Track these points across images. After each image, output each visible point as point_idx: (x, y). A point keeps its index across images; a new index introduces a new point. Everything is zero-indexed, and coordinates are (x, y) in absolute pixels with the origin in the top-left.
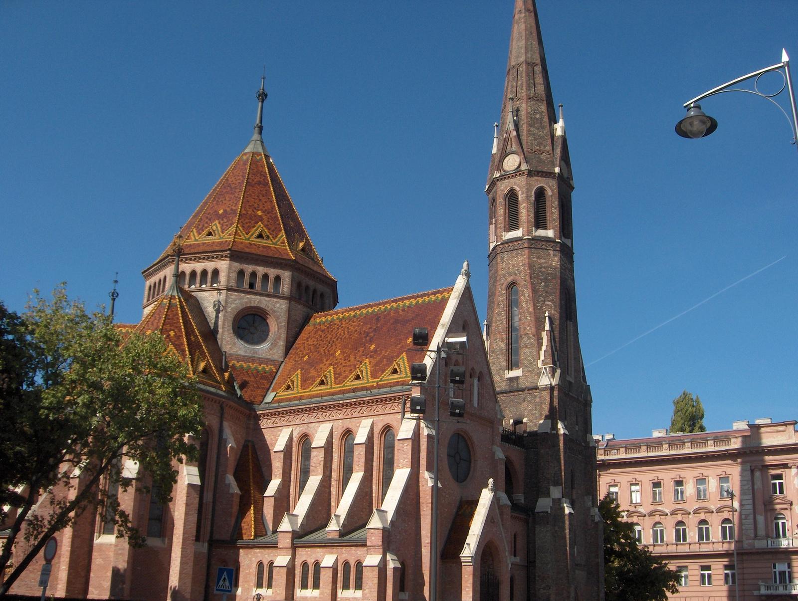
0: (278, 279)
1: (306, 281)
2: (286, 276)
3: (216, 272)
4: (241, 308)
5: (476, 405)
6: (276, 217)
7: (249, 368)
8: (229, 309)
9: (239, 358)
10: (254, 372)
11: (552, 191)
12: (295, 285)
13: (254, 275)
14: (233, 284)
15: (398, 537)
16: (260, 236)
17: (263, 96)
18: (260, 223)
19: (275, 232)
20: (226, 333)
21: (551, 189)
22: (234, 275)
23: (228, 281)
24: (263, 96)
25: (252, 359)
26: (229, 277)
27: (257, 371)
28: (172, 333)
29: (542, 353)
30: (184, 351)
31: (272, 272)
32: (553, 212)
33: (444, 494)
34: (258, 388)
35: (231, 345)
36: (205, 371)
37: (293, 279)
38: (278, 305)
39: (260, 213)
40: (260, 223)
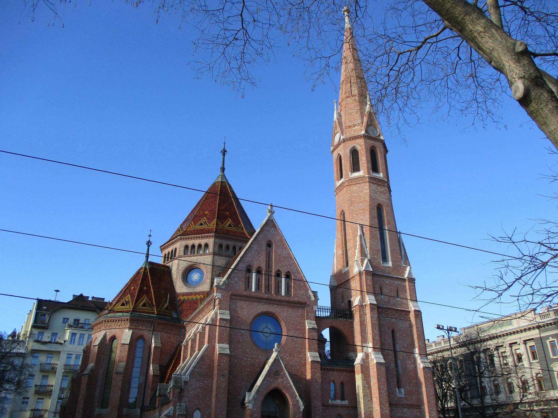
0: (207, 245)
1: (225, 243)
2: (211, 241)
3: (176, 249)
4: (186, 266)
5: (283, 294)
6: (215, 212)
7: (188, 299)
8: (180, 268)
9: (184, 294)
10: (190, 300)
11: (361, 146)
12: (217, 246)
13: (193, 246)
14: (182, 254)
15: (191, 393)
16: (201, 224)
17: (224, 152)
18: (205, 218)
19: (210, 220)
20: (178, 282)
21: (361, 145)
22: (182, 249)
23: (179, 253)
24: (224, 152)
25: (191, 294)
26: (179, 250)
27: (192, 299)
28: (133, 287)
29: (357, 251)
30: (134, 296)
31: (203, 242)
32: (363, 160)
33: (246, 359)
34: (190, 309)
35: (180, 287)
36: (144, 305)
37: (215, 243)
38: (207, 260)
39: (206, 212)
40: (205, 218)
